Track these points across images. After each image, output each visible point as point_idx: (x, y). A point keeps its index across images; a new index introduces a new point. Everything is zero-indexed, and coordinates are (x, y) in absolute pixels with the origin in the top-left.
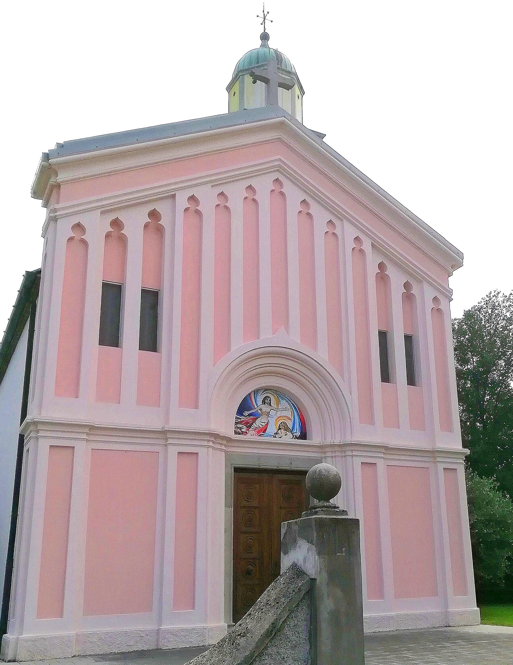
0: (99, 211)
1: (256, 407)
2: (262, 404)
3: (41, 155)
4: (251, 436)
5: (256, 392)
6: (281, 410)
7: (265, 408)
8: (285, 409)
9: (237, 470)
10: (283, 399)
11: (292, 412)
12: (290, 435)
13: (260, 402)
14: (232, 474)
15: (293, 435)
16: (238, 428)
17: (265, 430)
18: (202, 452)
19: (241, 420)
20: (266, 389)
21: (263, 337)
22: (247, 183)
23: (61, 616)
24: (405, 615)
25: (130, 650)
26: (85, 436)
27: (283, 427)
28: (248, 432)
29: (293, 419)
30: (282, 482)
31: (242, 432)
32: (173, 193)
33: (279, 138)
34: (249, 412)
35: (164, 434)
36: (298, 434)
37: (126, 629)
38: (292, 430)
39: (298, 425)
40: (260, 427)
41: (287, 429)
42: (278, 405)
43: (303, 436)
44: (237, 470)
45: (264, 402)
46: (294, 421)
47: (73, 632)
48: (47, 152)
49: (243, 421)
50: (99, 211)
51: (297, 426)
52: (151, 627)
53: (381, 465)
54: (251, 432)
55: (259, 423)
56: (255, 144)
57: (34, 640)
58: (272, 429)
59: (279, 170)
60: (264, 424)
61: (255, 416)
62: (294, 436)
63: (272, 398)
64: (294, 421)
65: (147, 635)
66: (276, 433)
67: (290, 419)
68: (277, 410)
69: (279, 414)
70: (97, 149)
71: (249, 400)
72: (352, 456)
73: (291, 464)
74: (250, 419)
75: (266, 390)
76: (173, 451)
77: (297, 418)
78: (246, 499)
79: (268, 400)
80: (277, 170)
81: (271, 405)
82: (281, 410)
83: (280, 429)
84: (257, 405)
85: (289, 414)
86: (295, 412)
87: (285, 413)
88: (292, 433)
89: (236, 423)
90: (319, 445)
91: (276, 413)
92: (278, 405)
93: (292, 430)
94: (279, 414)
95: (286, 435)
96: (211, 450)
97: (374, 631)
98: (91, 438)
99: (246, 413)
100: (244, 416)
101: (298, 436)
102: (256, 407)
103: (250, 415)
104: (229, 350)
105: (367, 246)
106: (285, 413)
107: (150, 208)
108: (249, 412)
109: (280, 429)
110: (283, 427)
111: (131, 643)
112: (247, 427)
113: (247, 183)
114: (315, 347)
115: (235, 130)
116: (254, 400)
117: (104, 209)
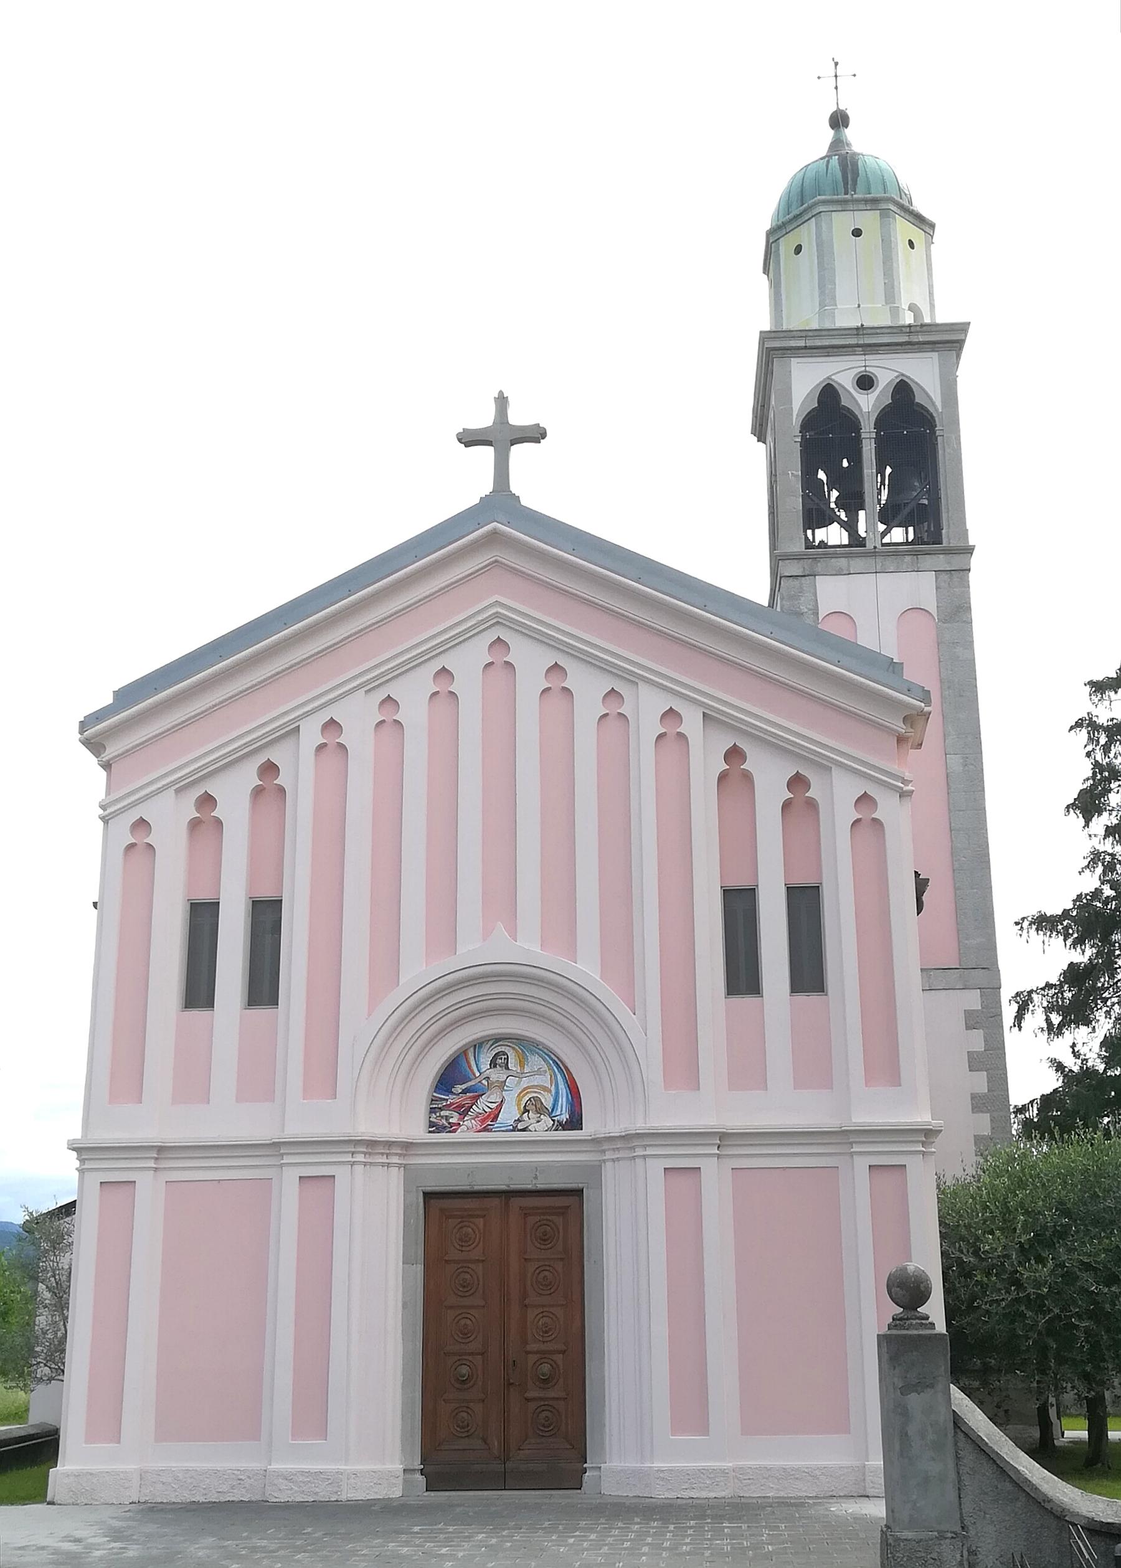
0: (172, 790)
1: (478, 1074)
2: (491, 1068)
3: (78, 724)
4: (467, 1131)
5: (477, 1045)
6: (528, 1075)
7: (497, 1075)
8: (539, 1072)
9: (428, 1196)
10: (532, 1052)
11: (551, 1076)
12: (547, 1121)
13: (485, 1064)
14: (418, 1203)
15: (553, 1121)
16: (442, 1117)
17: (496, 1117)
18: (341, 1174)
19: (449, 1103)
20: (498, 1039)
21: (461, 949)
22: (436, 666)
23: (119, 1442)
24: (760, 1468)
25: (222, 1499)
26: (151, 1164)
27: (534, 1106)
28: (461, 1123)
29: (553, 1092)
30: (526, 1213)
31: (449, 1123)
32: (297, 724)
33: (496, 561)
34: (464, 1086)
35: (276, 1147)
36: (565, 1117)
37: (219, 1465)
38: (553, 1110)
39: (564, 1099)
40: (486, 1112)
41: (541, 1110)
42: (522, 1066)
43: (575, 1122)
44: (428, 1196)
45: (493, 1064)
46: (557, 1093)
47: (132, 1467)
48: (83, 719)
49: (452, 1104)
50: (172, 790)
51: (563, 1101)
52: (256, 1465)
53: (709, 1167)
54: (468, 1122)
55: (483, 1105)
56: (444, 591)
57: (78, 1475)
58: (509, 1115)
59: (499, 621)
60: (493, 1106)
61: (476, 1094)
62: (556, 1122)
63: (511, 1054)
64: (557, 1093)
65: (249, 1477)
66: (519, 1120)
67: (550, 1091)
68: (520, 1076)
69: (525, 1083)
70: (157, 691)
71: (465, 1065)
72: (644, 1157)
73: (536, 1178)
74: (465, 1099)
75: (497, 1040)
76: (291, 1177)
77: (562, 1086)
78: (458, 1247)
79: (501, 1059)
80: (498, 623)
81: (507, 1068)
82: (528, 1075)
83: (526, 1111)
84: (479, 1071)
85: (545, 1080)
86: (559, 1076)
87: (537, 1080)
88: (551, 1118)
89: (432, 1110)
90: (590, 1138)
91: (519, 1083)
92: (522, 1066)
93: (553, 1110)
94: (525, 1083)
95: (538, 1122)
96: (359, 1169)
97: (679, 1496)
98: (164, 1164)
99: (459, 1088)
100: (455, 1094)
101: (565, 1120)
102: (478, 1074)
103: (464, 1092)
104: (398, 985)
105: (692, 724)
106: (537, 1080)
107: (261, 759)
108: (464, 1086)
109: (526, 1111)
110: (534, 1106)
111: (225, 1488)
112: (460, 1114)
113: (436, 666)
114: (571, 950)
115: (476, 539)
116: (473, 1063)
117: (177, 786)
